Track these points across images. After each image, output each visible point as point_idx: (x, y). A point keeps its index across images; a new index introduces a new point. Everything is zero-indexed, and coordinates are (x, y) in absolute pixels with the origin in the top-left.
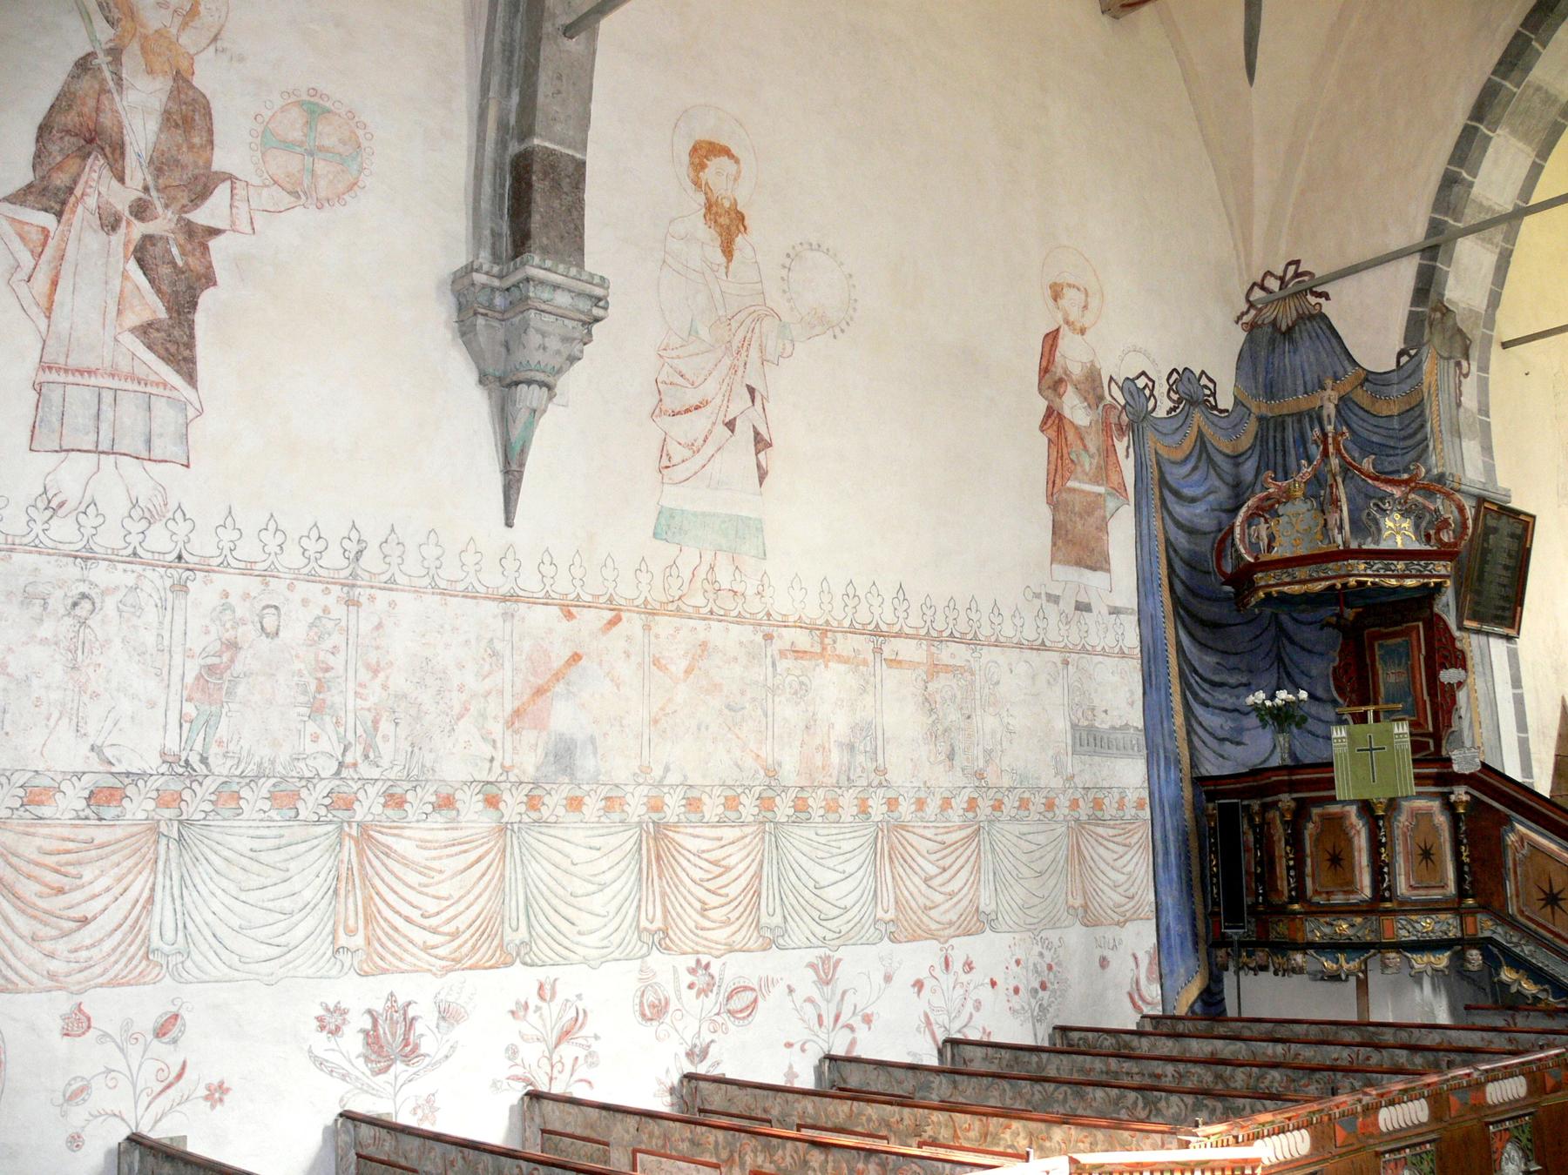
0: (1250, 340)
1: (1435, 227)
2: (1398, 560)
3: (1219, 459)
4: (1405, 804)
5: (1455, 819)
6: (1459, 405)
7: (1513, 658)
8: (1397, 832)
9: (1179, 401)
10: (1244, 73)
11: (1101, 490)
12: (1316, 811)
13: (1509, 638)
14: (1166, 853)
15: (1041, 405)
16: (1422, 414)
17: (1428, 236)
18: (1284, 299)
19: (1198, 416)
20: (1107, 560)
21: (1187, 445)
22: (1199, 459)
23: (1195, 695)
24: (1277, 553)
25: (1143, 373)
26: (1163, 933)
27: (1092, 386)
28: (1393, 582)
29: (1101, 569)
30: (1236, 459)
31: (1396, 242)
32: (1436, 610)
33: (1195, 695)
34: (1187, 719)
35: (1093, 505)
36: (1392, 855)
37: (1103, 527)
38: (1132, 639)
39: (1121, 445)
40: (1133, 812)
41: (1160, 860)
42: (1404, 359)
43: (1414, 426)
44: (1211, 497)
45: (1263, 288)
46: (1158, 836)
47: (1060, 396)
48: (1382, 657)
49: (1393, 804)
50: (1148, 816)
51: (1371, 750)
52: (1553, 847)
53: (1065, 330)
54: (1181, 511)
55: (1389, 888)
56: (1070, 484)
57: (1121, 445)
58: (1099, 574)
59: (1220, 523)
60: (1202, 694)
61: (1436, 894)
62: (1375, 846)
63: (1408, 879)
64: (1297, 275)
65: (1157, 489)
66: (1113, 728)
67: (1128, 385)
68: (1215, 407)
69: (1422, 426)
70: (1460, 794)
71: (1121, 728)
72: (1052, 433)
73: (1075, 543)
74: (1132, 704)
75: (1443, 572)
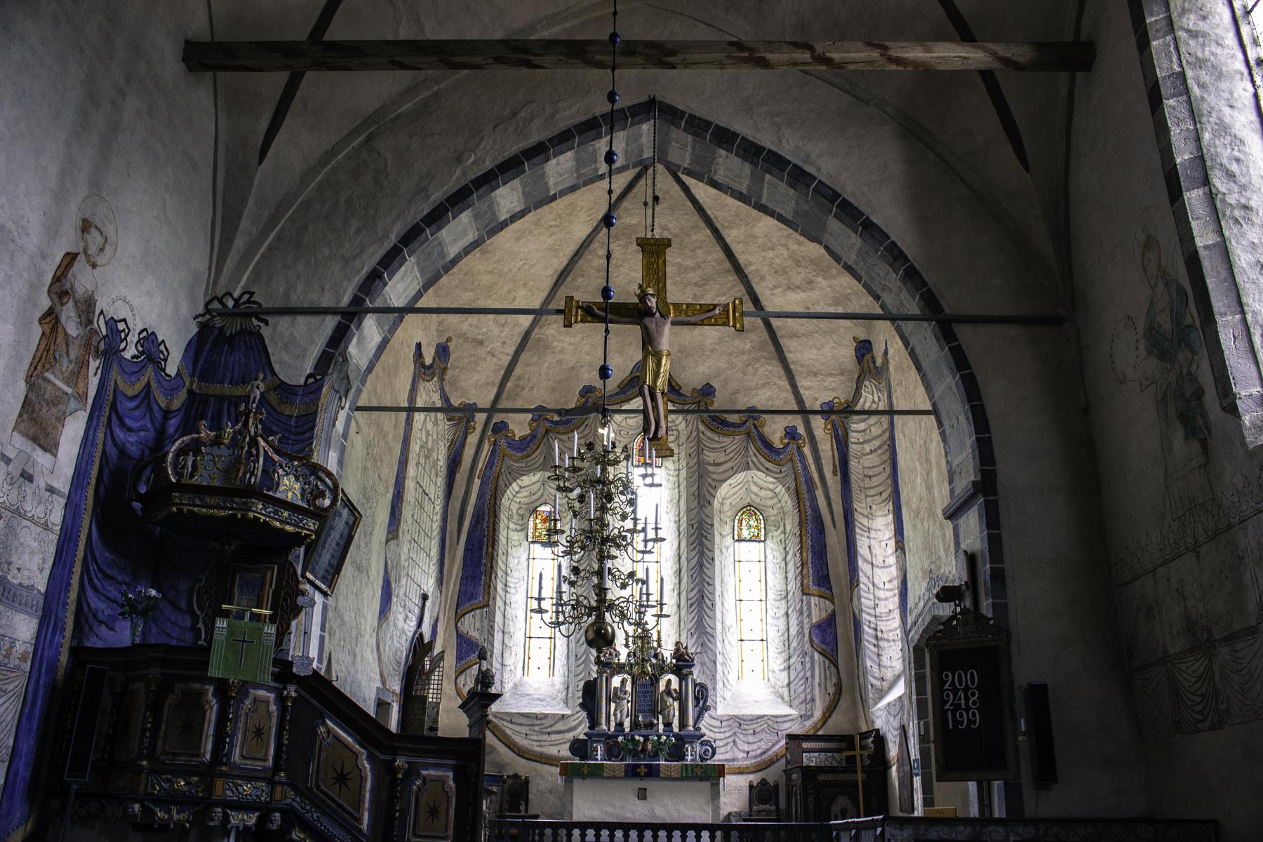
0: (199, 334)
1: (357, 301)
3: (156, 408)
6: (334, 425)
7: (325, 607)
9: (142, 353)
10: (257, 155)
11: (69, 390)
12: (179, 687)
13: (325, 594)
14: (34, 705)
15: (45, 303)
16: (315, 419)
17: (351, 304)
18: (233, 315)
19: (150, 370)
20: (56, 446)
21: (139, 387)
22: (143, 401)
23: (90, 580)
24: (196, 480)
25: (124, 320)
26: (11, 776)
27: (87, 308)
28: (278, 524)
29: (50, 452)
30: (167, 414)
31: (326, 302)
32: (290, 558)
33: (90, 580)
34: (79, 598)
35: (58, 399)
36: (235, 729)
37: (61, 420)
38: (57, 517)
39: (94, 364)
40: (17, 662)
41: (27, 710)
42: (311, 380)
43: (306, 427)
44: (142, 433)
45: (221, 302)
46: (31, 688)
47: (62, 304)
49: (244, 688)
50: (28, 669)
51: (244, 641)
52: (350, 739)
53: (81, 257)
54: (120, 434)
55: (226, 755)
56: (48, 375)
57: (94, 364)
58: (48, 455)
59: (143, 454)
60: (96, 581)
61: (258, 765)
63: (242, 750)
64: (248, 301)
65: (106, 410)
66: (21, 585)
67: (112, 323)
68: (164, 370)
69: (312, 428)
70: (292, 691)
71: (27, 587)
72: (47, 328)
73: (37, 424)
74: (41, 570)
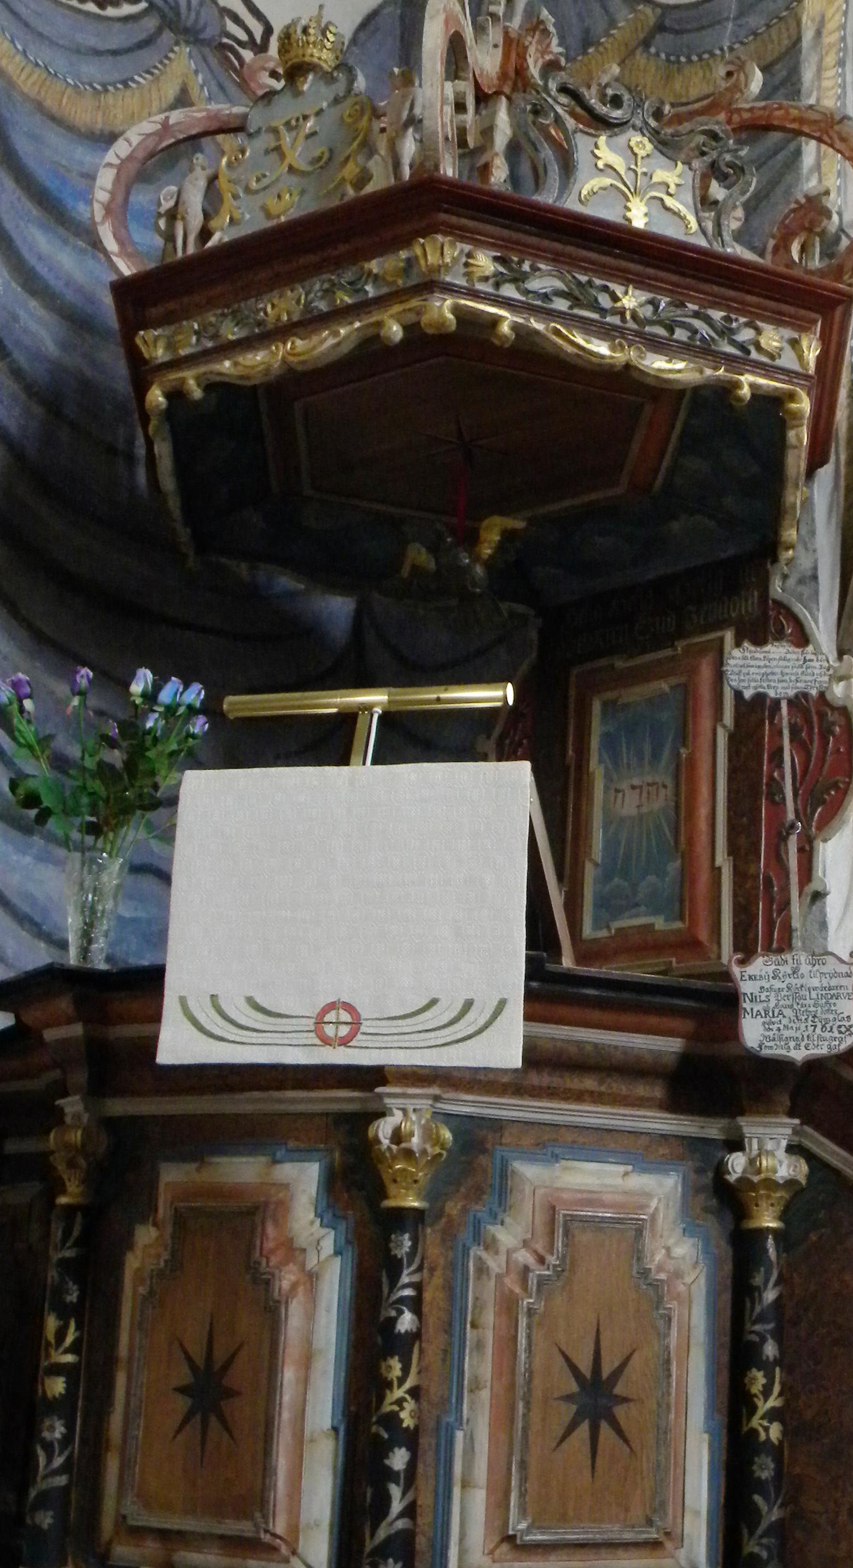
2: (628, 279)
4: (530, 1173)
5: (743, 1248)
8: (483, 1296)
12: (173, 1176)
28: (601, 348)
32: (777, 588)
48: (609, 742)
62: (372, 1341)
63: (499, 1504)
70: (772, 1151)
75: (788, 360)
